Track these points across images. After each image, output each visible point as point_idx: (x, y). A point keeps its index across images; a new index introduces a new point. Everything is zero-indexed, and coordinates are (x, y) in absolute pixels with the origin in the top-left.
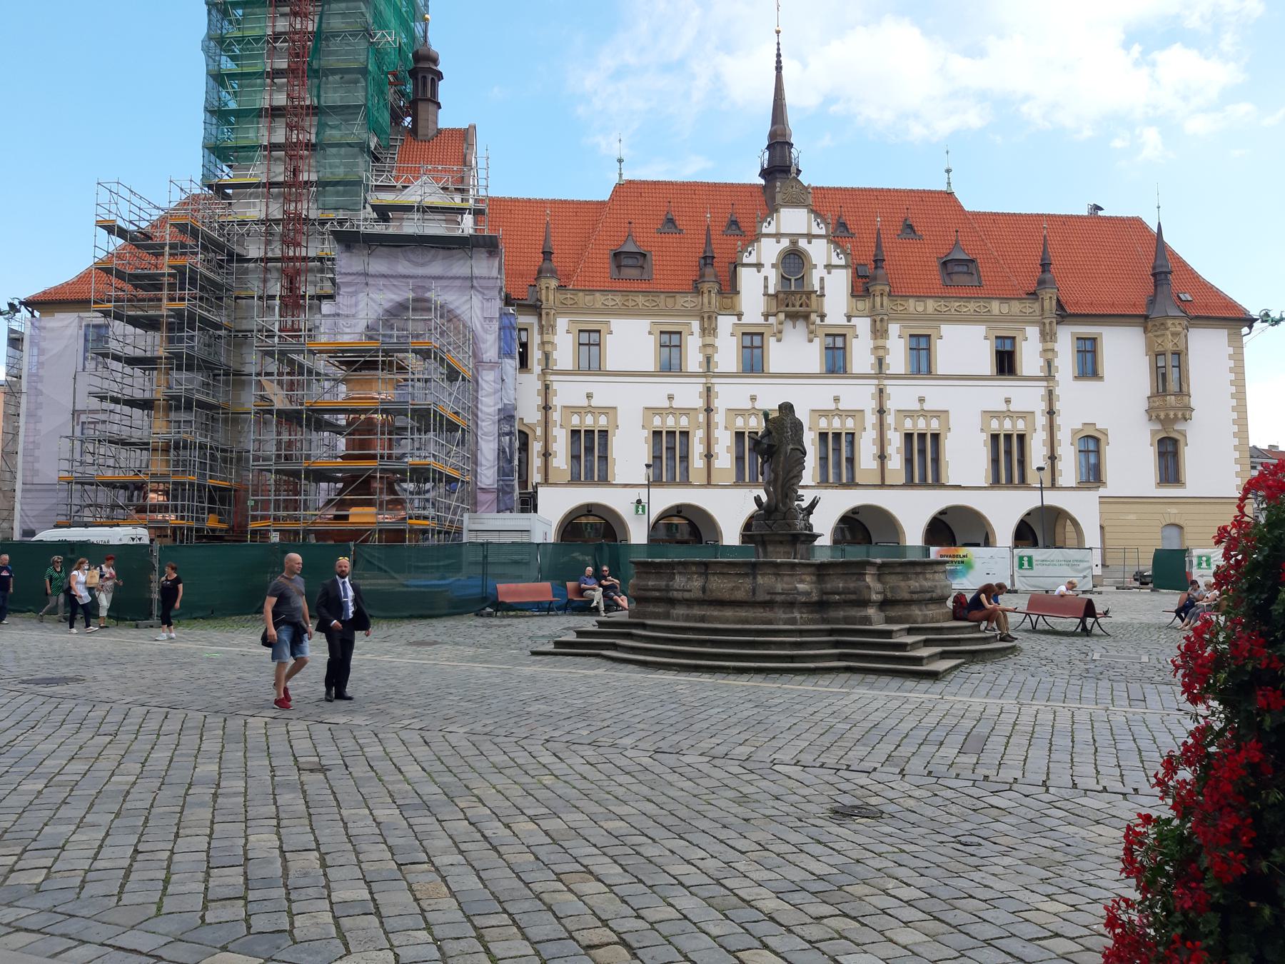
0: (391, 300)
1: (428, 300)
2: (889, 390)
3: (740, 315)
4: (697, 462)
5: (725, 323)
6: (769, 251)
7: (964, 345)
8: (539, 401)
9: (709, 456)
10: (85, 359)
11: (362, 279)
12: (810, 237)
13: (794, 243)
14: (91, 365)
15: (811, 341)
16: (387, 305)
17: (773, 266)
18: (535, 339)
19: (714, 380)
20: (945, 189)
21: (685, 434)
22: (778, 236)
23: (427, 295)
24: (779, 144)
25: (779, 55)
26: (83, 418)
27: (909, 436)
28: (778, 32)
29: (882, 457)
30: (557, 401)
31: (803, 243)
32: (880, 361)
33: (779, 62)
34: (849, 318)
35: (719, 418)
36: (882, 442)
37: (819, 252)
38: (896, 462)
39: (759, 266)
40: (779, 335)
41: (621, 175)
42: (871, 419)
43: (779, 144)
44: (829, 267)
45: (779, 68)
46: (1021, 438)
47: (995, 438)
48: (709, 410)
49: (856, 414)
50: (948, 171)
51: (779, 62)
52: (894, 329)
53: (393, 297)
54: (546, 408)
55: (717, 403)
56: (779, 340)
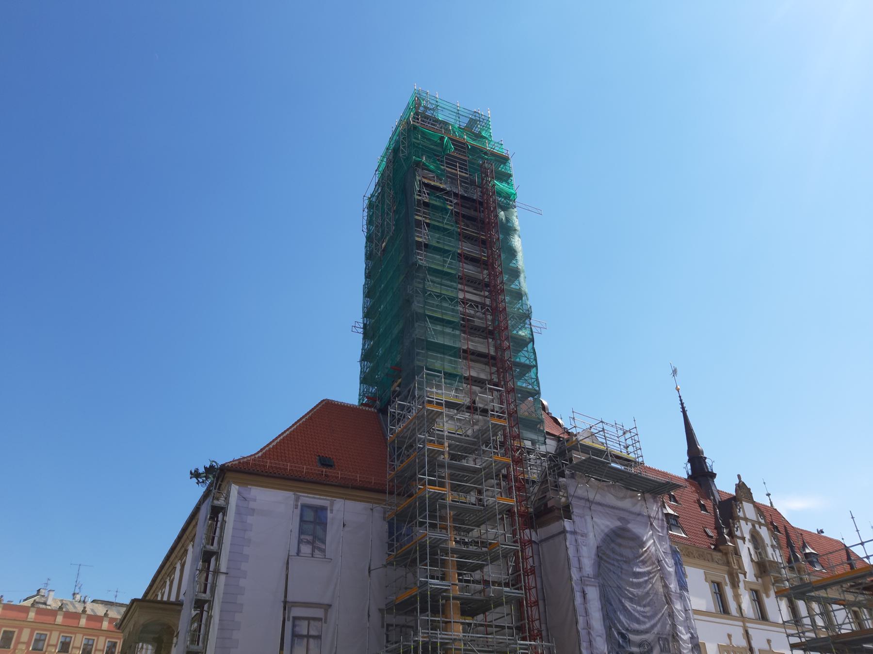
0: (607, 526)
1: (628, 530)
10: (300, 542)
11: (588, 504)
14: (306, 549)
16: (606, 530)
19: (748, 625)
22: (746, 519)
23: (630, 526)
24: (695, 457)
25: (682, 404)
26: (296, 612)
31: (757, 526)
33: (683, 408)
43: (695, 457)
50: (768, 495)
51: (683, 408)
53: (609, 523)
55: (754, 645)
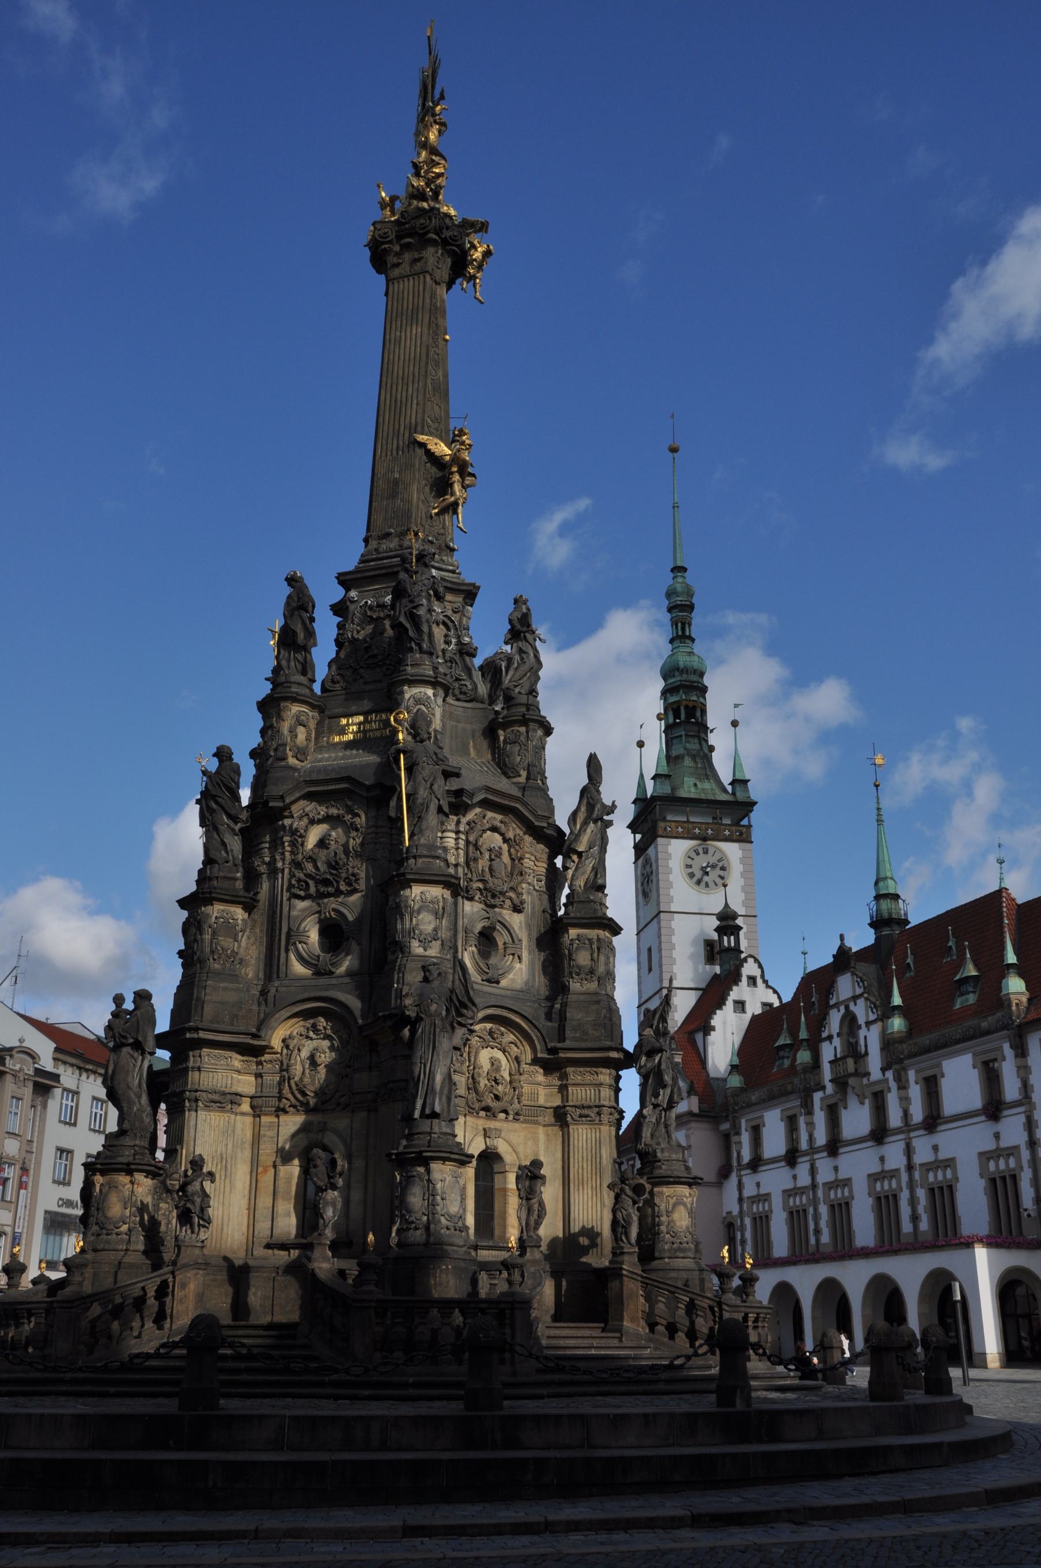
2: (915, 1143)
3: (824, 1088)
4: (812, 1240)
5: (817, 1096)
6: (835, 1019)
7: (960, 1080)
8: (736, 1195)
9: (817, 1232)
12: (855, 998)
13: (847, 1008)
15: (862, 1103)
17: (839, 1035)
18: (734, 1139)
20: (997, 888)
21: (805, 1211)
22: (837, 1005)
25: (878, 809)
27: (932, 1190)
28: (877, 786)
29: (915, 1218)
30: (747, 1193)
31: (852, 1007)
32: (906, 1114)
34: (883, 1070)
35: (820, 1193)
36: (913, 1201)
37: (861, 1011)
38: (924, 1225)
39: (830, 1038)
40: (844, 1100)
41: (805, 968)
42: (904, 1177)
44: (868, 1024)
45: (880, 821)
46: (1014, 1177)
47: (993, 1181)
48: (814, 1186)
49: (894, 1174)
52: (912, 1075)
54: (741, 1200)
56: (846, 1108)
